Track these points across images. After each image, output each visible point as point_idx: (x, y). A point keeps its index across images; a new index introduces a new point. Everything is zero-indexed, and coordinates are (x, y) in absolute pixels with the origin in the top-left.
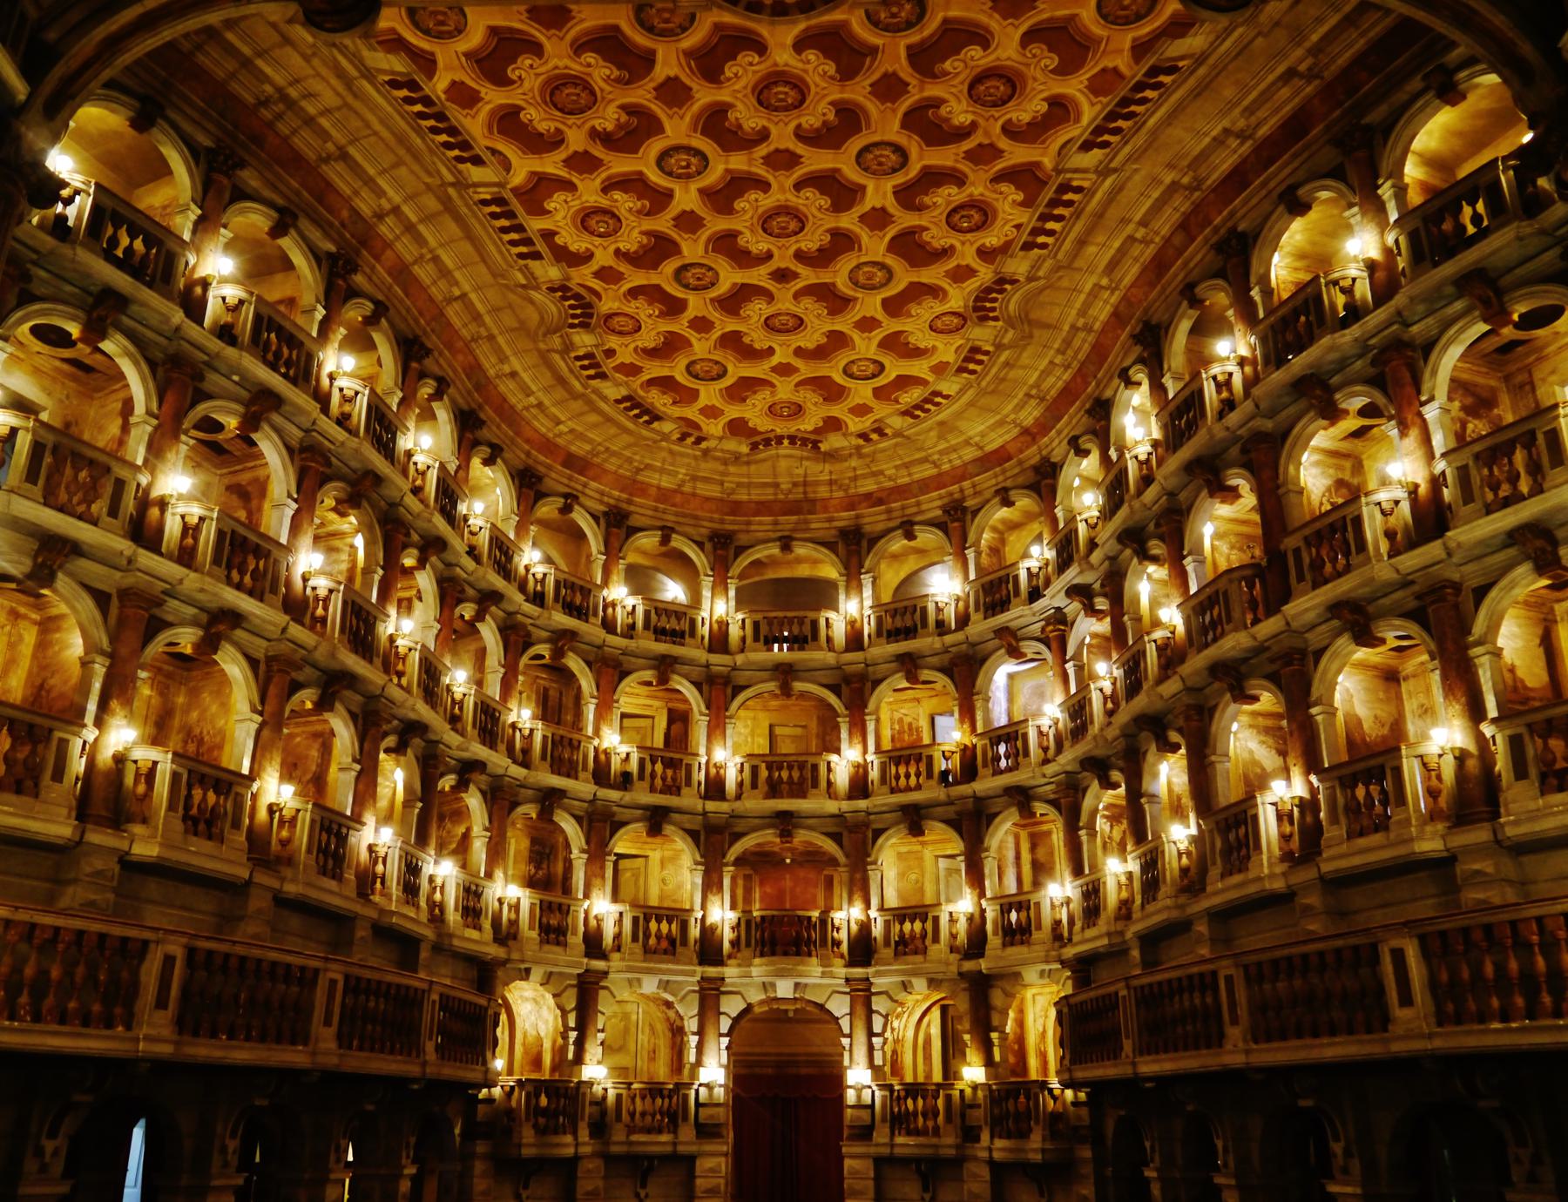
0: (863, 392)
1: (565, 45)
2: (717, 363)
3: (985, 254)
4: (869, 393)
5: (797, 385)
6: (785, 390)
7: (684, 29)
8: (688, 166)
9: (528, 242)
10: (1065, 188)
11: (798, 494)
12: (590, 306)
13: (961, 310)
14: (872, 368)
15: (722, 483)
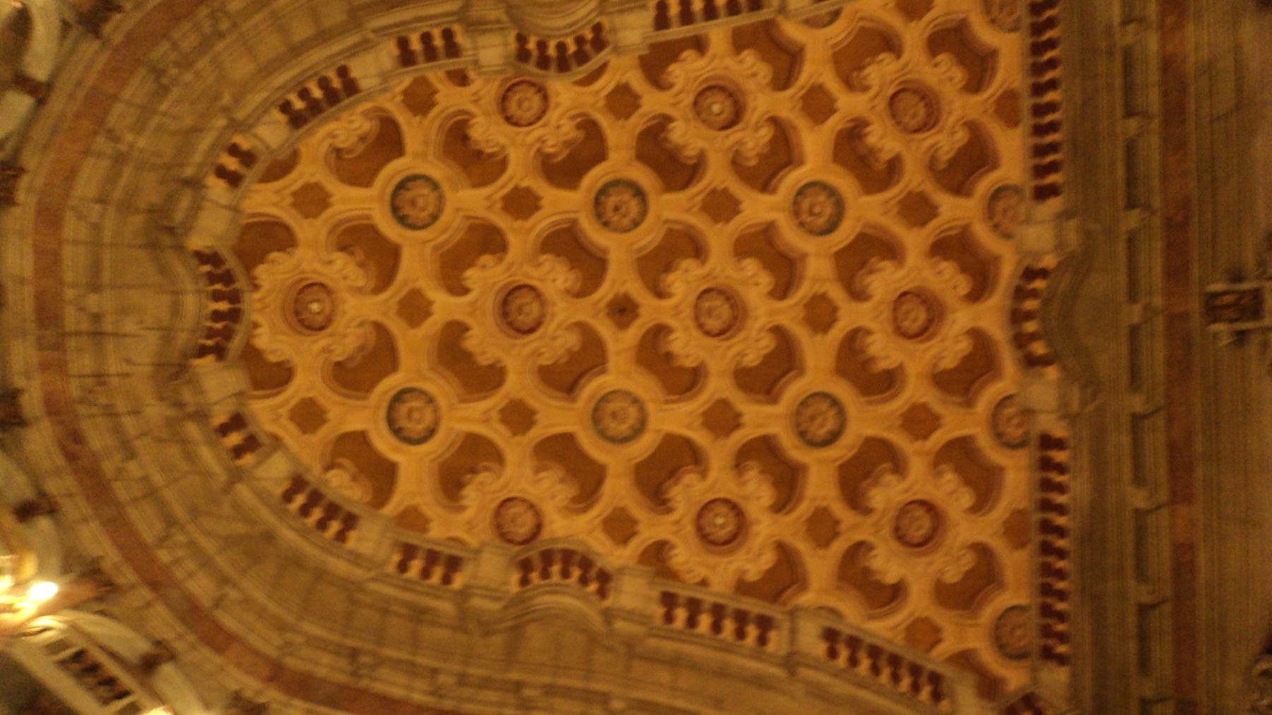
1: (973, 114)
2: (435, 217)
3: (657, 555)
4: (354, 423)
5: (380, 328)
7: (996, 226)
8: (811, 213)
9: (687, 17)
10: (765, 624)
11: (72, 318)
12: (563, 65)
13: (545, 534)
14: (415, 428)
15: (102, 200)
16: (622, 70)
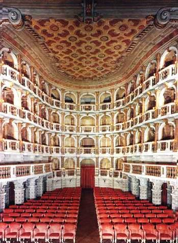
0: (100, 72)
3: (120, 53)
6: (88, 71)
16: (57, 55)
